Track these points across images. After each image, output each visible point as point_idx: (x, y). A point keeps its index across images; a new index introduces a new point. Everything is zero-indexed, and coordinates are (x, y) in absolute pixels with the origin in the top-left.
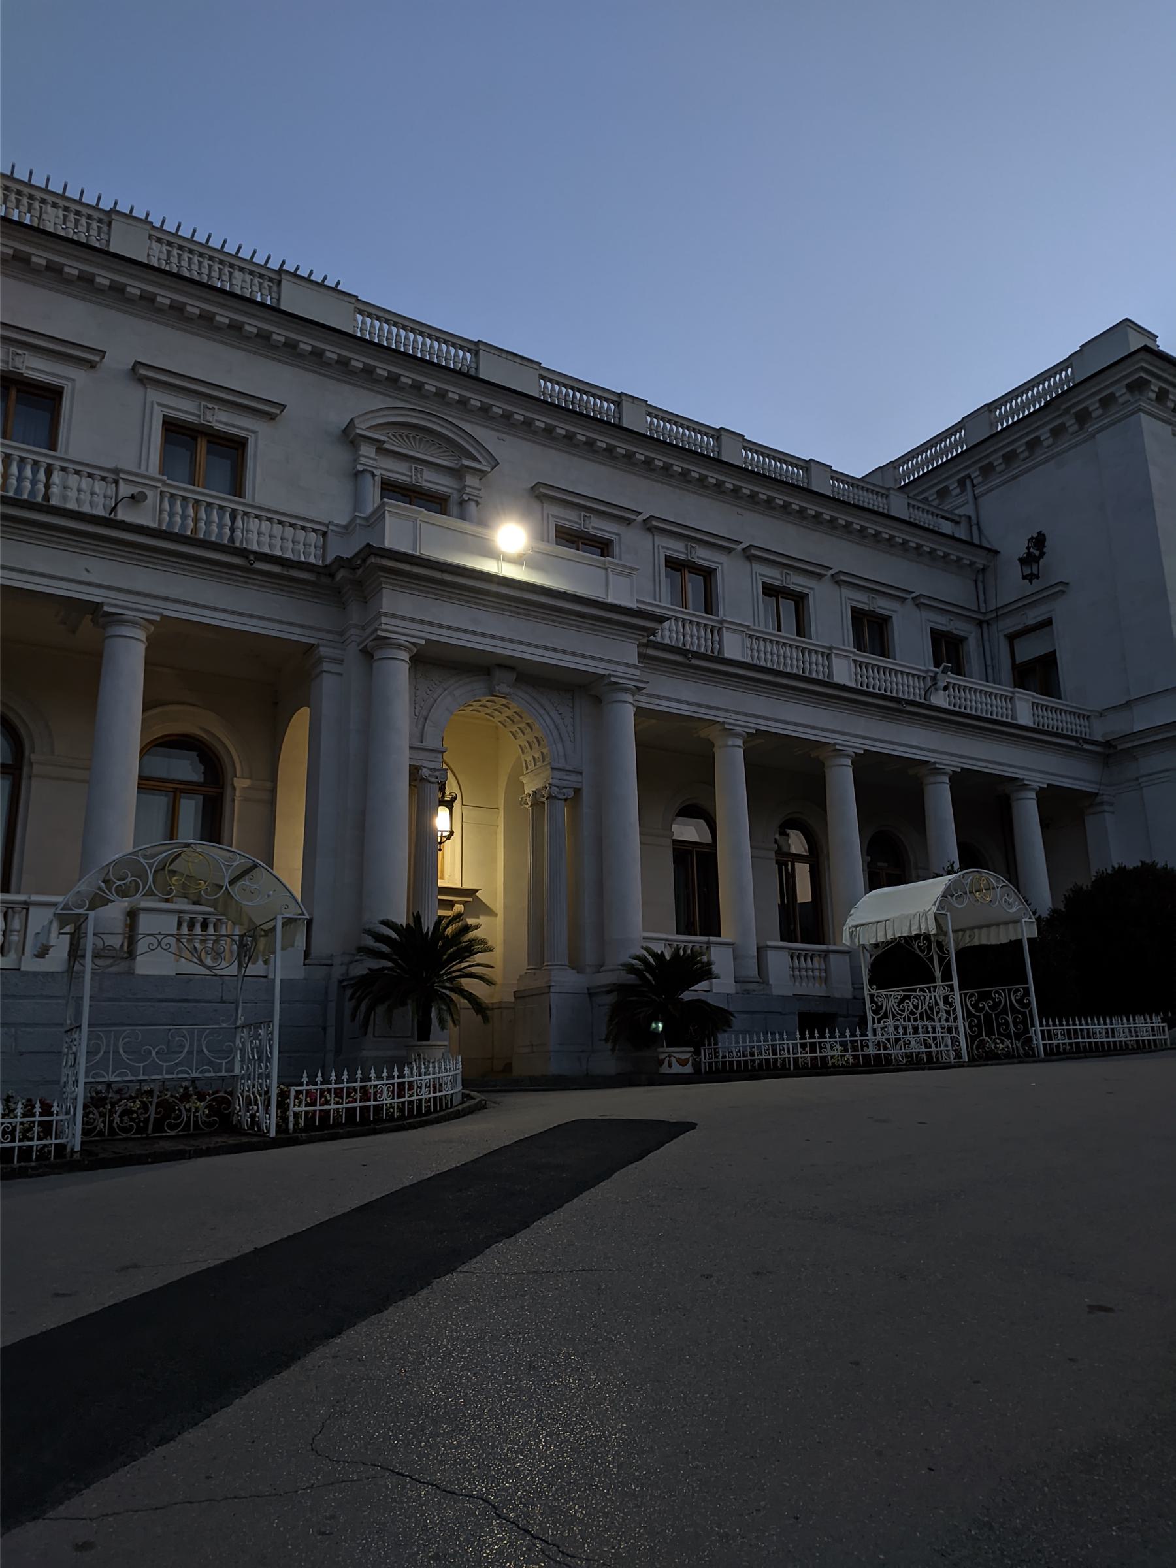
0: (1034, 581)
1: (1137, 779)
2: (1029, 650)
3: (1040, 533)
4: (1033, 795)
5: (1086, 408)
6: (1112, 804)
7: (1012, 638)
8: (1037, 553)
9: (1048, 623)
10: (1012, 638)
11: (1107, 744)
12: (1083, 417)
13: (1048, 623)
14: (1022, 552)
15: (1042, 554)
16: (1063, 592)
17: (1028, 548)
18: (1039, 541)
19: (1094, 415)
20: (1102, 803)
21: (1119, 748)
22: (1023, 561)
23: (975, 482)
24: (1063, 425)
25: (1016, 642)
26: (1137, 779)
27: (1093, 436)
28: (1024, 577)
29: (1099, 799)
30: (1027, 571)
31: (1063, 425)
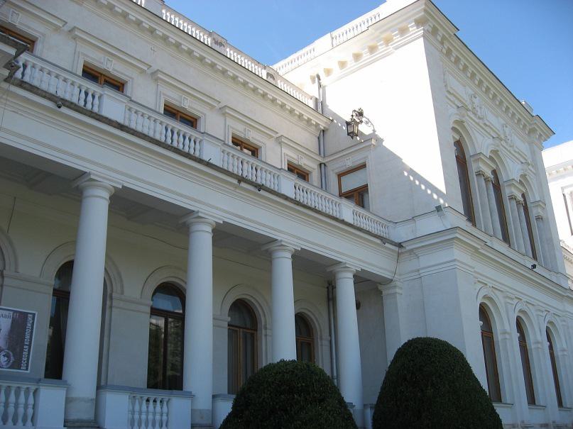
1: (418, 270)
2: (351, 183)
4: (351, 275)
6: (401, 288)
7: (340, 176)
9: (363, 166)
10: (340, 176)
11: (400, 245)
18: (361, 114)
20: (395, 287)
21: (407, 248)
29: (393, 284)
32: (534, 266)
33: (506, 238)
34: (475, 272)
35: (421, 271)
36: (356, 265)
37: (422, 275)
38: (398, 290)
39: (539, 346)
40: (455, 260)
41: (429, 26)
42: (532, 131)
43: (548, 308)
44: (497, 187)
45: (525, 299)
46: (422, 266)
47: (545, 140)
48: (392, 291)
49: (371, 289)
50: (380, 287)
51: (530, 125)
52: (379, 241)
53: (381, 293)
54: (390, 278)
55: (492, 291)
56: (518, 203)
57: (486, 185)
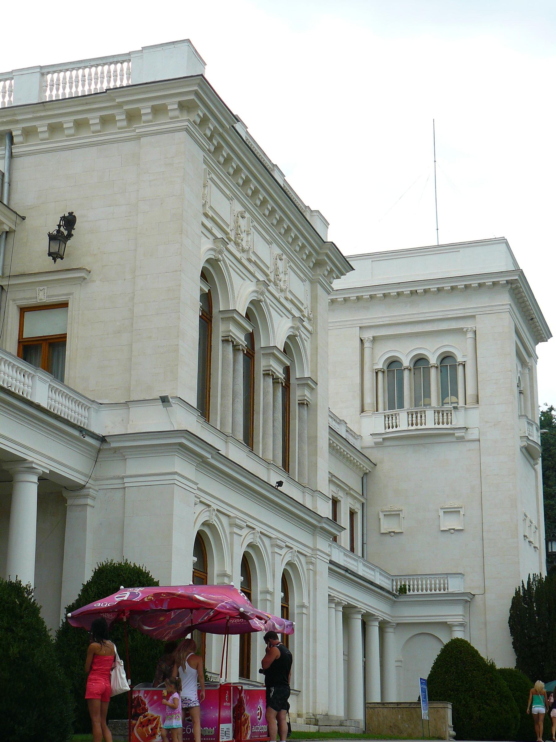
0: (58, 260)
1: (123, 478)
2: (40, 327)
3: (71, 214)
4: (35, 479)
5: (139, 110)
6: (94, 498)
7: (23, 310)
8: (66, 233)
9: (64, 305)
10: (23, 310)
11: (103, 439)
12: (133, 117)
13: (64, 305)
14: (53, 229)
15: (70, 235)
16: (85, 279)
17: (59, 226)
19: (144, 118)
20: (87, 496)
21: (113, 445)
22: (52, 238)
23: (15, 140)
24: (113, 117)
25: (27, 315)
26: (123, 478)
27: (138, 137)
28: (50, 254)
29: (84, 491)
30: (55, 248)
31: (113, 117)
32: (280, 484)
33: (249, 439)
34: (199, 489)
35: (126, 480)
36: (44, 465)
37: (126, 485)
38: (89, 501)
39: (269, 597)
40: (176, 473)
41: (198, 115)
42: (318, 264)
43: (290, 543)
44: (250, 356)
45: (259, 528)
46: (128, 473)
47: (338, 278)
48: (82, 501)
49: (56, 496)
50: (65, 494)
51: (318, 253)
52: (76, 433)
53: (65, 501)
54: (83, 483)
55: (216, 515)
56: (276, 381)
57: (234, 355)
